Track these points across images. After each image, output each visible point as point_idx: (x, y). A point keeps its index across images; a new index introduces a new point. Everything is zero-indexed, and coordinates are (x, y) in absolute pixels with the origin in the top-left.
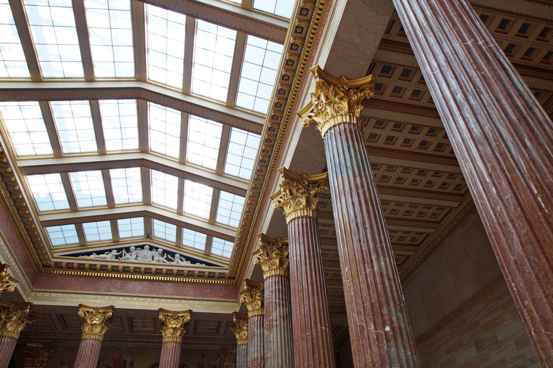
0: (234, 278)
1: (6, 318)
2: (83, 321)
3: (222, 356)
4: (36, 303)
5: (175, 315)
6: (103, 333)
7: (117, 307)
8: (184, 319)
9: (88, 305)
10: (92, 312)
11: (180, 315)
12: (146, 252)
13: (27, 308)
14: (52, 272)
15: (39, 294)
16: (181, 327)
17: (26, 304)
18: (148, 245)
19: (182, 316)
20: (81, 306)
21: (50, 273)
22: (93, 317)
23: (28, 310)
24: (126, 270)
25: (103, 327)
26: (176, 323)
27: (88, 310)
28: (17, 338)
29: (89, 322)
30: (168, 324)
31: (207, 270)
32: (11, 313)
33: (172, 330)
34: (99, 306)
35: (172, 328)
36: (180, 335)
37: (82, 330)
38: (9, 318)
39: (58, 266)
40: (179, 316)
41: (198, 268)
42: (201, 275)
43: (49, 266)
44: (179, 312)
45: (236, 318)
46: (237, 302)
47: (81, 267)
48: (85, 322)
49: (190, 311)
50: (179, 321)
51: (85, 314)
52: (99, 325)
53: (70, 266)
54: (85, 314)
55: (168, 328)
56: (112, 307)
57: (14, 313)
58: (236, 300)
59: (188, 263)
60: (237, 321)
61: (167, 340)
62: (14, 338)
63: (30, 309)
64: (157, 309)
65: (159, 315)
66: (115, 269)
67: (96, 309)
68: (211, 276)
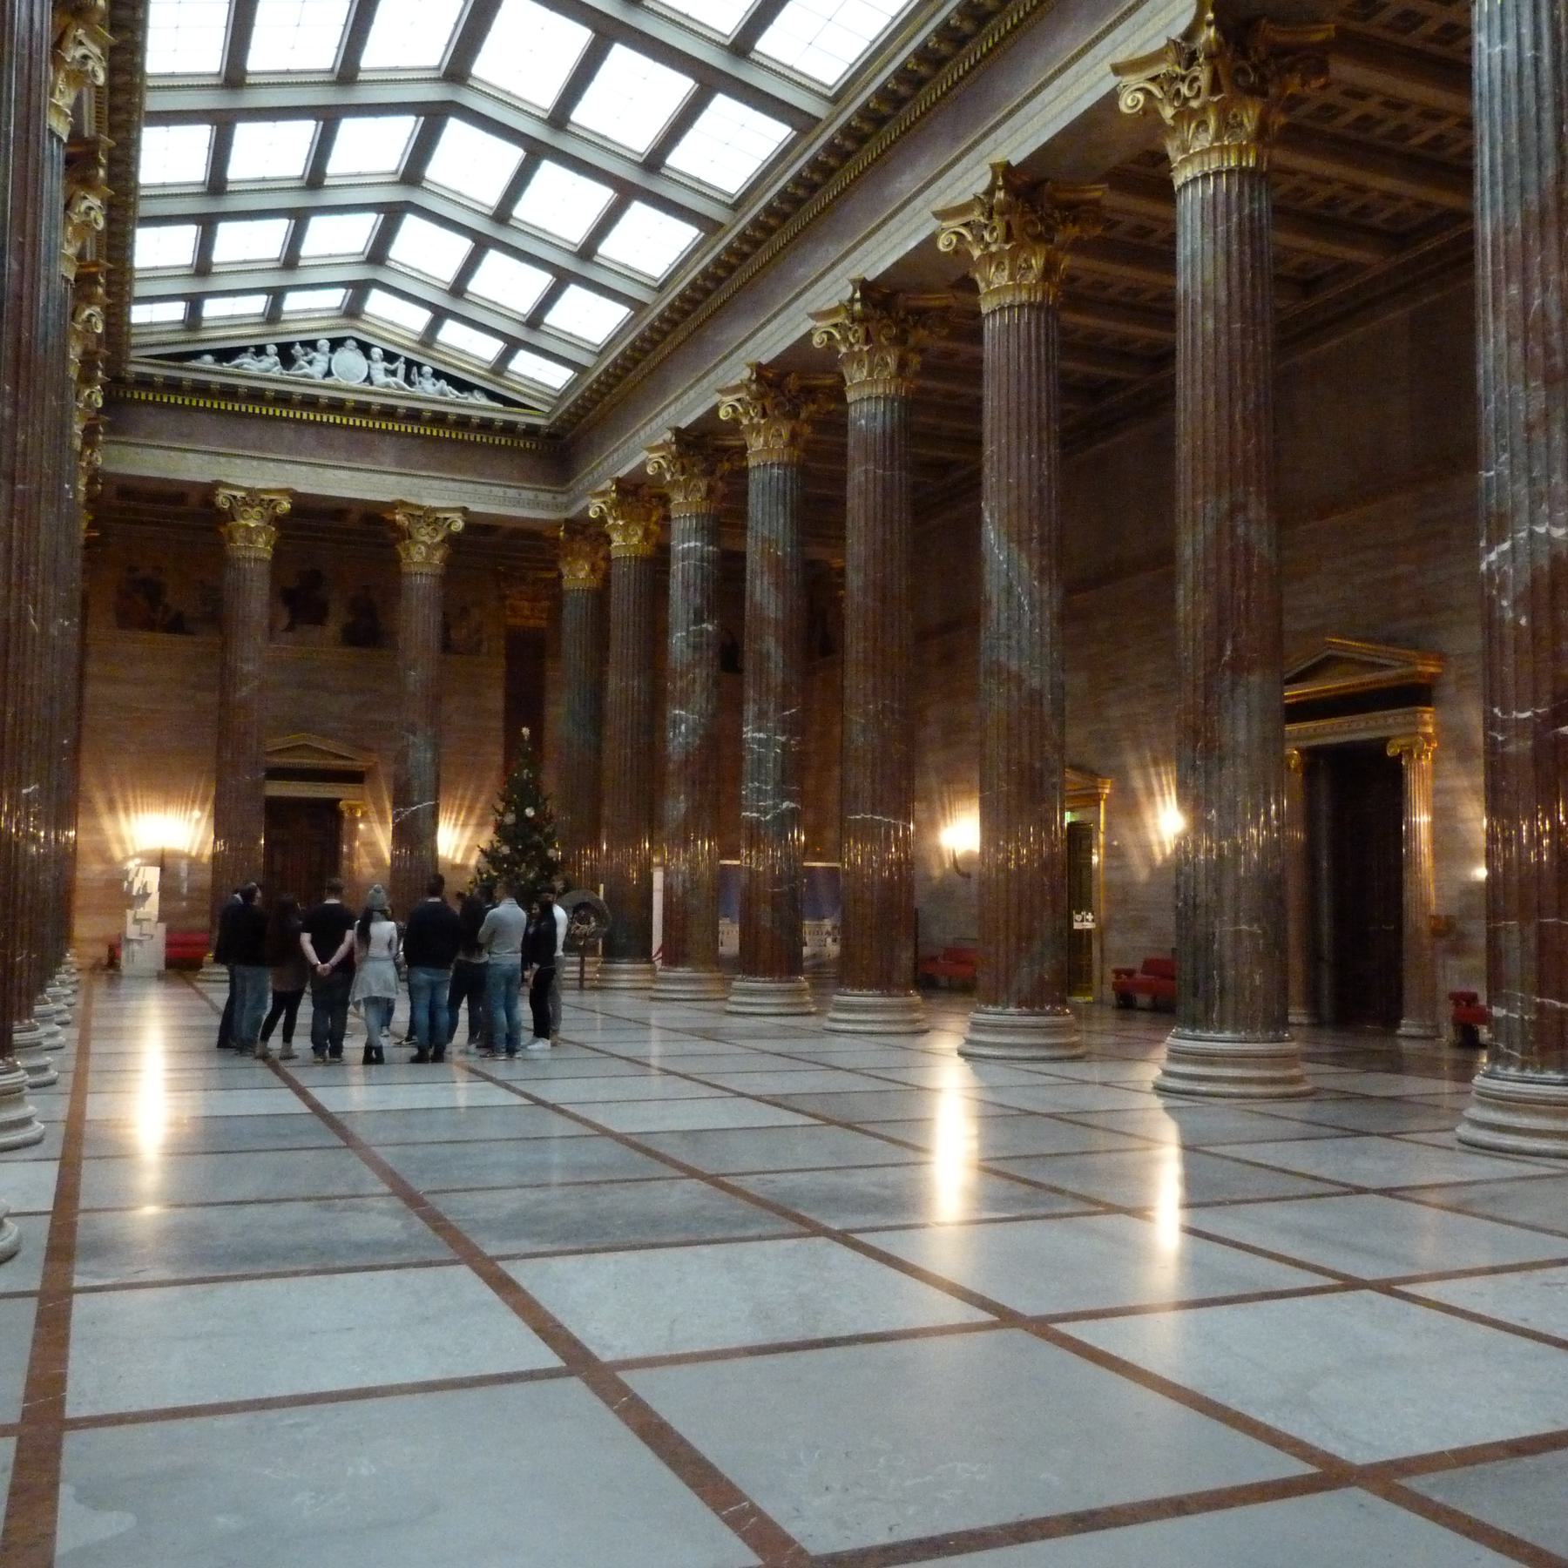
4: (111, 468)
5: (429, 516)
7: (300, 489)
8: (449, 526)
9: (230, 481)
11: (441, 515)
16: (443, 541)
18: (357, 341)
19: (446, 519)
20: (217, 484)
24: (310, 403)
27: (235, 493)
30: (415, 535)
31: (500, 414)
34: (260, 485)
35: (424, 543)
39: (145, 382)
41: (477, 405)
42: (486, 425)
45: (565, 531)
46: (563, 493)
47: (202, 389)
49: (464, 510)
53: (173, 386)
55: (417, 542)
59: (452, 393)
61: (414, 569)
66: (283, 399)
68: (509, 428)
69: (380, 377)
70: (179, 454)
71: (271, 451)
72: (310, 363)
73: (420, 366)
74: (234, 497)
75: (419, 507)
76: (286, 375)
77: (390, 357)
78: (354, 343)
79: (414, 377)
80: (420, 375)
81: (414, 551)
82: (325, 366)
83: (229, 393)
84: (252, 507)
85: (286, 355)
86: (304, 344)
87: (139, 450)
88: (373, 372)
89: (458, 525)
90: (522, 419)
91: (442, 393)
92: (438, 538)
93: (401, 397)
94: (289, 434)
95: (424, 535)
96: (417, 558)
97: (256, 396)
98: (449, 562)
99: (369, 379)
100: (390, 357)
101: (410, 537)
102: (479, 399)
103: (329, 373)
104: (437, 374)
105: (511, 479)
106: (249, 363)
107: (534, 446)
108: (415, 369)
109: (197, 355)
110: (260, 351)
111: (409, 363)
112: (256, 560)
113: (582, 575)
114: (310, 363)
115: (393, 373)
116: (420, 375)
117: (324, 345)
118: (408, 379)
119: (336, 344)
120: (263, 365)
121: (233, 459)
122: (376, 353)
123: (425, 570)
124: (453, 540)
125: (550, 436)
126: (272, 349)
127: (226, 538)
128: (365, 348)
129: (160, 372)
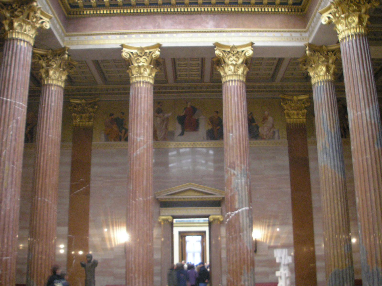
0: (300, 4)
1: (47, 66)
2: (127, 63)
3: (282, 104)
4: (72, 47)
6: (154, 75)
7: (164, 45)
8: (245, 54)
10: (137, 53)
11: (240, 50)
13: (64, 53)
14: (82, 13)
15: (75, 39)
16: (242, 63)
17: (63, 50)
19: (243, 51)
20: (123, 46)
21: (80, 14)
22: (138, 59)
23: (66, 56)
25: (152, 69)
26: (236, 59)
27: (132, 51)
28: (63, 85)
29: (136, 65)
30: (226, 60)
32: (50, 60)
33: (232, 68)
34: (144, 46)
35: (232, 64)
36: (243, 73)
37: (128, 74)
38: (50, 66)
40: (238, 52)
43: (77, 7)
45: (309, 50)
46: (305, 32)
48: (131, 64)
49: (252, 44)
50: (239, 56)
51: (130, 56)
52: (148, 67)
54: (130, 56)
55: (228, 65)
56: (159, 46)
57: (53, 60)
58: (305, 30)
60: (312, 55)
61: (228, 78)
62: (60, 87)
63: (69, 55)
64: (211, 44)
65: (215, 50)
67: (141, 49)
70: (106, 36)
74: (132, 53)
81: (226, 69)
84: (141, 57)
87: (86, 37)
89: (249, 52)
92: (241, 61)
95: (231, 60)
101: (225, 62)
107: (287, 10)
112: (143, 82)
113: (322, 73)
121: (131, 35)
123: (235, 78)
124: (248, 62)
125: (294, 4)
127: (130, 75)
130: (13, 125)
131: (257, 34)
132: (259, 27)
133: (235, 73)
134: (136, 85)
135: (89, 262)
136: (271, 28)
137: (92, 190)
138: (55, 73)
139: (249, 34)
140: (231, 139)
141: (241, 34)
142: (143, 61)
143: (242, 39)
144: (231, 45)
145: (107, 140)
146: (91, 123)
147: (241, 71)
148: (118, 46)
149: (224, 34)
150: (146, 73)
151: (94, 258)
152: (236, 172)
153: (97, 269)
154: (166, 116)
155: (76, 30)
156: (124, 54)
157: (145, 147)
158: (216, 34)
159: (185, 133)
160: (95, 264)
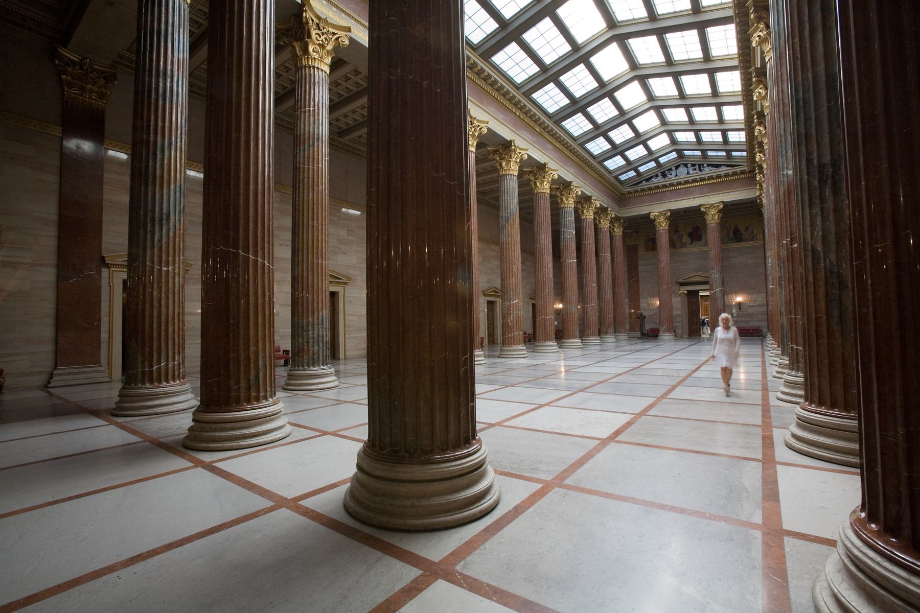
2: (654, 220)
4: (624, 216)
6: (668, 224)
12: (682, 171)
13: (621, 220)
15: (625, 211)
16: (718, 212)
20: (650, 213)
31: (730, 170)
33: (711, 216)
36: (718, 218)
41: (723, 170)
42: (727, 175)
43: (624, 194)
44: (714, 204)
47: (643, 190)
49: (723, 202)
53: (636, 191)
59: (714, 169)
61: (709, 222)
62: (620, 235)
66: (664, 186)
68: (735, 174)
69: (691, 171)
71: (671, 199)
72: (671, 174)
73: (703, 165)
75: (709, 204)
76: (664, 180)
77: (693, 165)
78: (682, 165)
79: (702, 168)
80: (703, 167)
81: (708, 217)
82: (675, 174)
83: (650, 189)
85: (664, 175)
86: (668, 170)
88: (689, 171)
90: (738, 170)
91: (711, 170)
92: (717, 211)
93: (698, 175)
94: (668, 194)
96: (710, 219)
97: (657, 187)
98: (722, 219)
99: (688, 173)
100: (693, 165)
102: (725, 168)
103: (676, 175)
104: (708, 165)
105: (738, 188)
106: (654, 180)
108: (702, 166)
109: (641, 182)
110: (657, 176)
111: (699, 165)
114: (671, 174)
115: (695, 169)
116: (703, 167)
117: (674, 168)
118: (700, 170)
119: (677, 167)
120: (658, 179)
122: (689, 165)
124: (720, 211)
125: (750, 172)
126: (660, 174)
128: (686, 165)
129: (631, 189)
130: (606, 264)
131: (726, 194)
132: (727, 190)
133: (713, 219)
134: (659, 232)
135: (642, 316)
136: (735, 189)
137: (640, 279)
138: (617, 229)
139: (721, 195)
140: (711, 255)
141: (716, 196)
142: (662, 219)
143: (716, 199)
144: (710, 203)
145: (646, 251)
146: (636, 243)
147: (716, 218)
148: (648, 212)
149: (706, 197)
150: (664, 225)
151: (644, 314)
152: (714, 271)
153: (646, 320)
154: (681, 233)
155: (625, 206)
156: (651, 216)
157: (666, 262)
158: (701, 198)
159: (693, 242)
160: (645, 317)
